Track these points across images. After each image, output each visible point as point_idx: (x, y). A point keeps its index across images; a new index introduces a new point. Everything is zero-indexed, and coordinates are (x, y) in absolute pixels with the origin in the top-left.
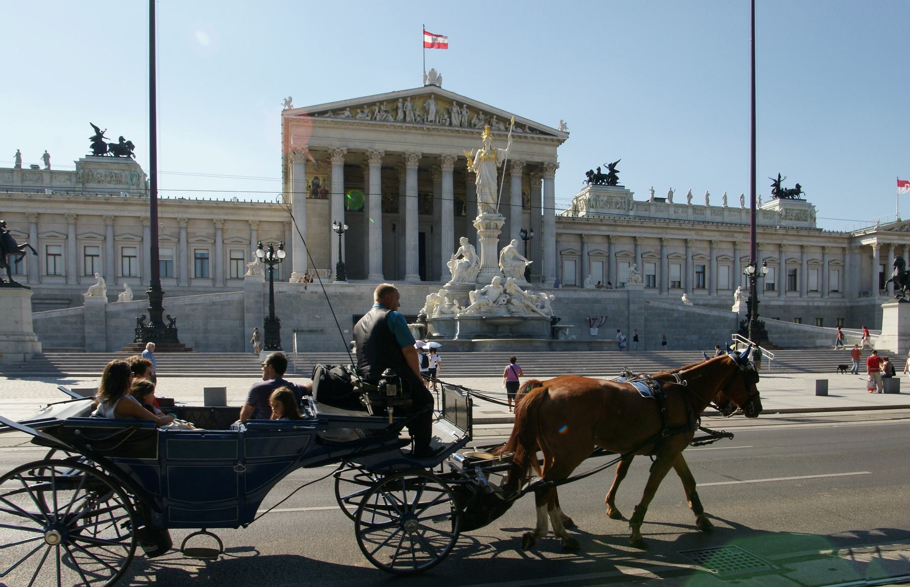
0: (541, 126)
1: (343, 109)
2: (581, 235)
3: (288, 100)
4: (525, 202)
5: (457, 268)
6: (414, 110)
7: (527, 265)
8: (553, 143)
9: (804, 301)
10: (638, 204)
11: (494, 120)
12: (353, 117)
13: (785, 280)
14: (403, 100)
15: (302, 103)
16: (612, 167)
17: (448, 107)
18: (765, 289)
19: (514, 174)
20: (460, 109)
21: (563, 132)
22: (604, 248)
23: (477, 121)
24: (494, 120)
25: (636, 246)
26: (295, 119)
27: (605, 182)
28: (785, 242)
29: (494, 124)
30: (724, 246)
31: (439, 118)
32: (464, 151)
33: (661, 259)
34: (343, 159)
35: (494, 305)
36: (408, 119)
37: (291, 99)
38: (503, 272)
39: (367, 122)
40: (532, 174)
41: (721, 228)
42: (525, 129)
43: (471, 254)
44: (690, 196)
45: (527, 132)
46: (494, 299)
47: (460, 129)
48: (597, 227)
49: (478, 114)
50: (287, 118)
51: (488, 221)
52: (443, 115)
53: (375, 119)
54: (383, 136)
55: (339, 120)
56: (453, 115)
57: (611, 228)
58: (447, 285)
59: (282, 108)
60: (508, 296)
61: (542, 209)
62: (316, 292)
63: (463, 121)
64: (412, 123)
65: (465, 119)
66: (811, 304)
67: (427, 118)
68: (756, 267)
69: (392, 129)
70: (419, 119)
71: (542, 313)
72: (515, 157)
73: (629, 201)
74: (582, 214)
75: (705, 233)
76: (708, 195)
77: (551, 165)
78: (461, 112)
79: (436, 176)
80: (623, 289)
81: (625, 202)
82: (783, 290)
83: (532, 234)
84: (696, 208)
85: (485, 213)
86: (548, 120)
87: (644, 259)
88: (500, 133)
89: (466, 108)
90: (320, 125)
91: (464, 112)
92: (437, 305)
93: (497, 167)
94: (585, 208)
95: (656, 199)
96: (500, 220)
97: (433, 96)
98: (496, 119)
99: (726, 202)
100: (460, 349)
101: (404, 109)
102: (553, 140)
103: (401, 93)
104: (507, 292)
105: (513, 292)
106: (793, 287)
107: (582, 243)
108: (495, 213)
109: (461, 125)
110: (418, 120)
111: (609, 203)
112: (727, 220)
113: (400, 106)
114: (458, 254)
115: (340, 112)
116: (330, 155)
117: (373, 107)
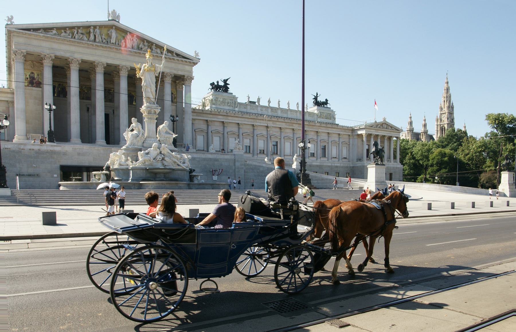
0: (183, 53)
1: (52, 29)
2: (207, 120)
3: (10, 17)
4: (173, 99)
5: (130, 137)
6: (101, 35)
7: (174, 137)
8: (190, 64)
9: (329, 163)
10: (241, 104)
11: (154, 47)
12: (59, 35)
13: (320, 152)
14: (94, 28)
15: (21, 20)
16: (225, 81)
17: (124, 35)
18: (310, 156)
19: (166, 81)
20: (132, 37)
21: (197, 58)
22: (220, 129)
23: (143, 46)
25: (239, 128)
26: (15, 31)
27: (221, 90)
28: (320, 130)
29: (154, 49)
30: (288, 131)
31: (118, 42)
32: (134, 64)
33: (253, 136)
34: (51, 62)
35: (154, 161)
36: (97, 40)
37: (12, 17)
38: (159, 140)
39: (68, 39)
40: (177, 82)
41: (286, 121)
43: (139, 129)
44: (269, 102)
45: (174, 56)
46: (154, 157)
47: (132, 50)
48: (217, 116)
49: (144, 42)
50: (9, 30)
51: (149, 109)
52: (121, 40)
53: (75, 38)
54: (81, 50)
55: (48, 36)
56: (127, 41)
57: (225, 117)
58: (124, 147)
59: (6, 23)
60: (162, 155)
61: (184, 104)
62: (33, 150)
63: (134, 45)
64: (100, 43)
65: (135, 45)
66: (333, 165)
67: (110, 41)
68: (304, 143)
69: (86, 45)
70: (104, 41)
71: (183, 166)
72: (167, 71)
73: (235, 102)
74: (207, 108)
75: (278, 123)
76: (279, 101)
77: (189, 77)
78: (133, 39)
79: (116, 78)
80: (231, 153)
81: (233, 102)
82: (319, 157)
83: (177, 118)
84: (273, 109)
85: (148, 104)
86: (188, 50)
87: (244, 136)
88: (157, 55)
89: (136, 37)
90: (35, 37)
91: (135, 40)
92: (117, 160)
93: (156, 76)
94: (209, 104)
95: (250, 102)
96: (157, 109)
97: (114, 27)
98: (155, 46)
99: (289, 106)
100: (133, 188)
101: (95, 34)
102: (190, 62)
103: (92, 23)
104: (162, 153)
105: (166, 153)
106: (324, 155)
107: (208, 125)
108: (154, 104)
109: (132, 48)
110: (104, 42)
111: (223, 102)
112: (289, 116)
114: (130, 128)
115: (50, 30)
116: (42, 58)
117: (73, 30)
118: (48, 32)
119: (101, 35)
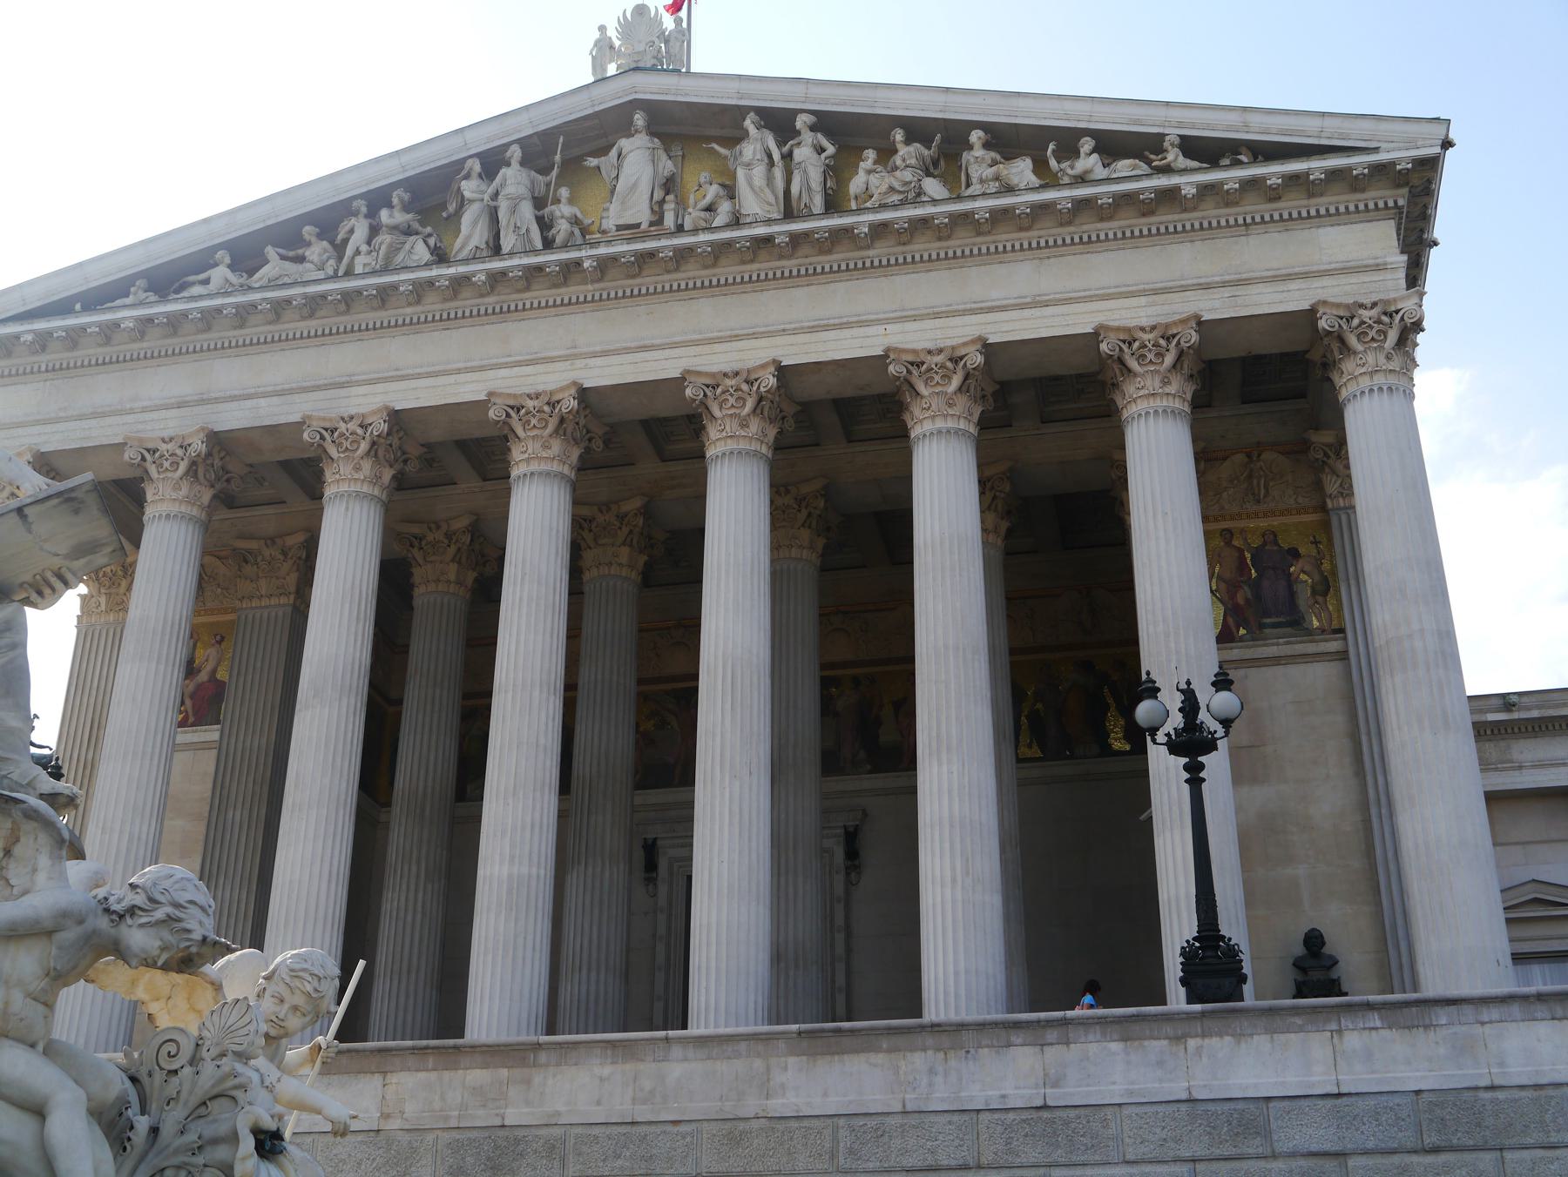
0: (1254, 120)
1: (200, 263)
20: (781, 143)
24: (978, 152)
29: (976, 174)
36: (508, 242)
42: (1166, 158)
54: (400, 351)
56: (740, 173)
63: (795, 189)
70: (562, 229)
77: (1365, 314)
83: (1225, 701)
91: (803, 153)
97: (639, 119)
98: (987, 146)
110: (559, 240)
113: (467, 194)
115: (191, 278)
118: (193, 284)
119: (539, 203)
